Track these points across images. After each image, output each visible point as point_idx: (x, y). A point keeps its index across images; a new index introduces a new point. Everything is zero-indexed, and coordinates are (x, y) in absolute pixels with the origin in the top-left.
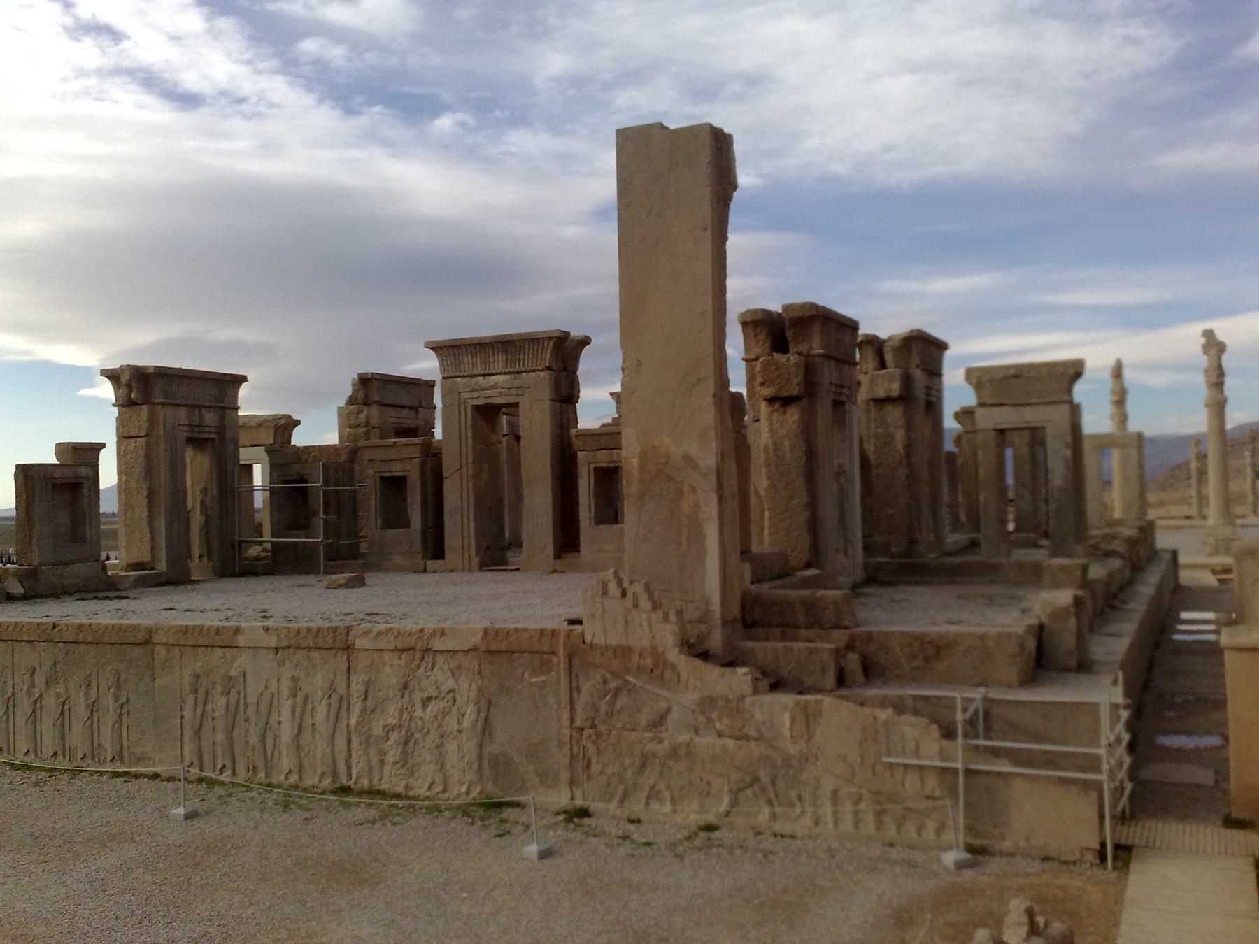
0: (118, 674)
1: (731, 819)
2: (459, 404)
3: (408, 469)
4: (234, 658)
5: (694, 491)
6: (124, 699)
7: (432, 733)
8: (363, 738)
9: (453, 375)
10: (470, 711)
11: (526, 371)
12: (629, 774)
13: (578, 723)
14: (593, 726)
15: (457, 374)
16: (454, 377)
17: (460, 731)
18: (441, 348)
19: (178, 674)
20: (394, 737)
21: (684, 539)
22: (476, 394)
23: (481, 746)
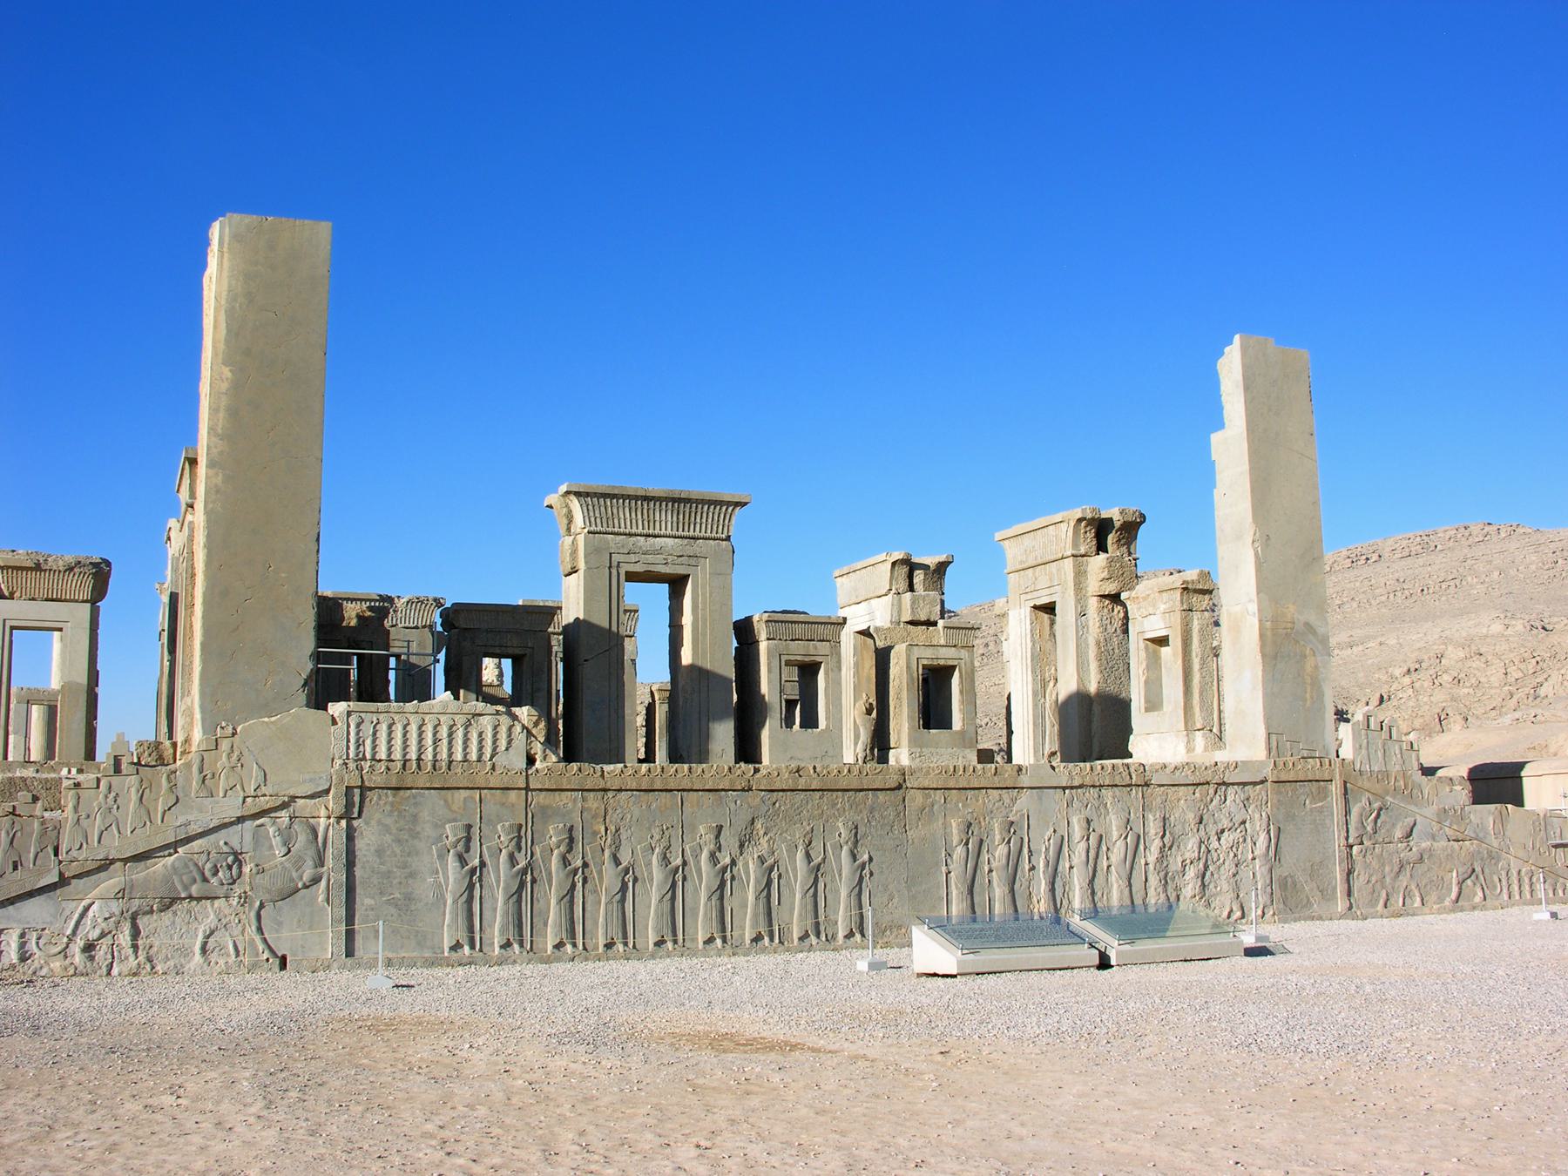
0: (856, 827)
1: (1460, 904)
2: (610, 567)
3: (530, 645)
4: (1013, 801)
5: (1314, 655)
6: (866, 857)
7: (1226, 864)
8: (1162, 874)
9: (603, 530)
10: (1262, 840)
11: (703, 538)
12: (1388, 880)
13: (1351, 841)
14: (1362, 843)
15: (610, 530)
16: (604, 533)
17: (1254, 859)
18: (587, 494)
19: (940, 823)
20: (1191, 872)
21: (1308, 696)
22: (633, 558)
23: (1271, 871)
